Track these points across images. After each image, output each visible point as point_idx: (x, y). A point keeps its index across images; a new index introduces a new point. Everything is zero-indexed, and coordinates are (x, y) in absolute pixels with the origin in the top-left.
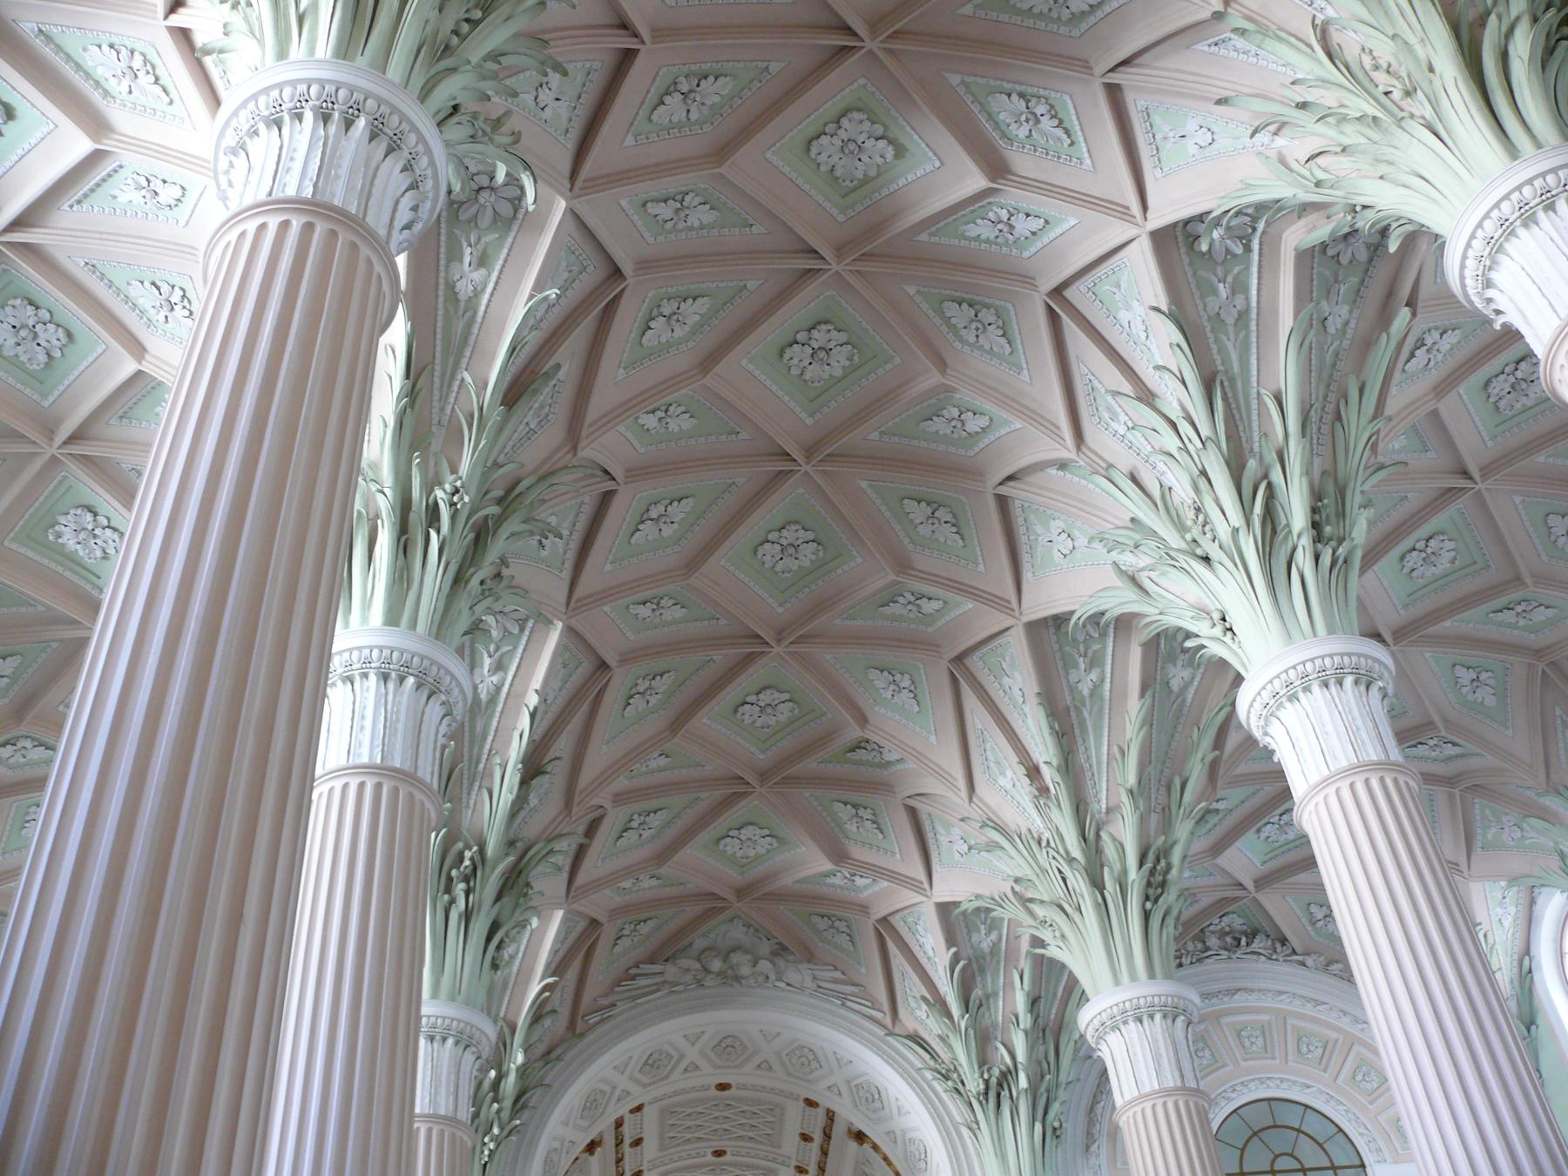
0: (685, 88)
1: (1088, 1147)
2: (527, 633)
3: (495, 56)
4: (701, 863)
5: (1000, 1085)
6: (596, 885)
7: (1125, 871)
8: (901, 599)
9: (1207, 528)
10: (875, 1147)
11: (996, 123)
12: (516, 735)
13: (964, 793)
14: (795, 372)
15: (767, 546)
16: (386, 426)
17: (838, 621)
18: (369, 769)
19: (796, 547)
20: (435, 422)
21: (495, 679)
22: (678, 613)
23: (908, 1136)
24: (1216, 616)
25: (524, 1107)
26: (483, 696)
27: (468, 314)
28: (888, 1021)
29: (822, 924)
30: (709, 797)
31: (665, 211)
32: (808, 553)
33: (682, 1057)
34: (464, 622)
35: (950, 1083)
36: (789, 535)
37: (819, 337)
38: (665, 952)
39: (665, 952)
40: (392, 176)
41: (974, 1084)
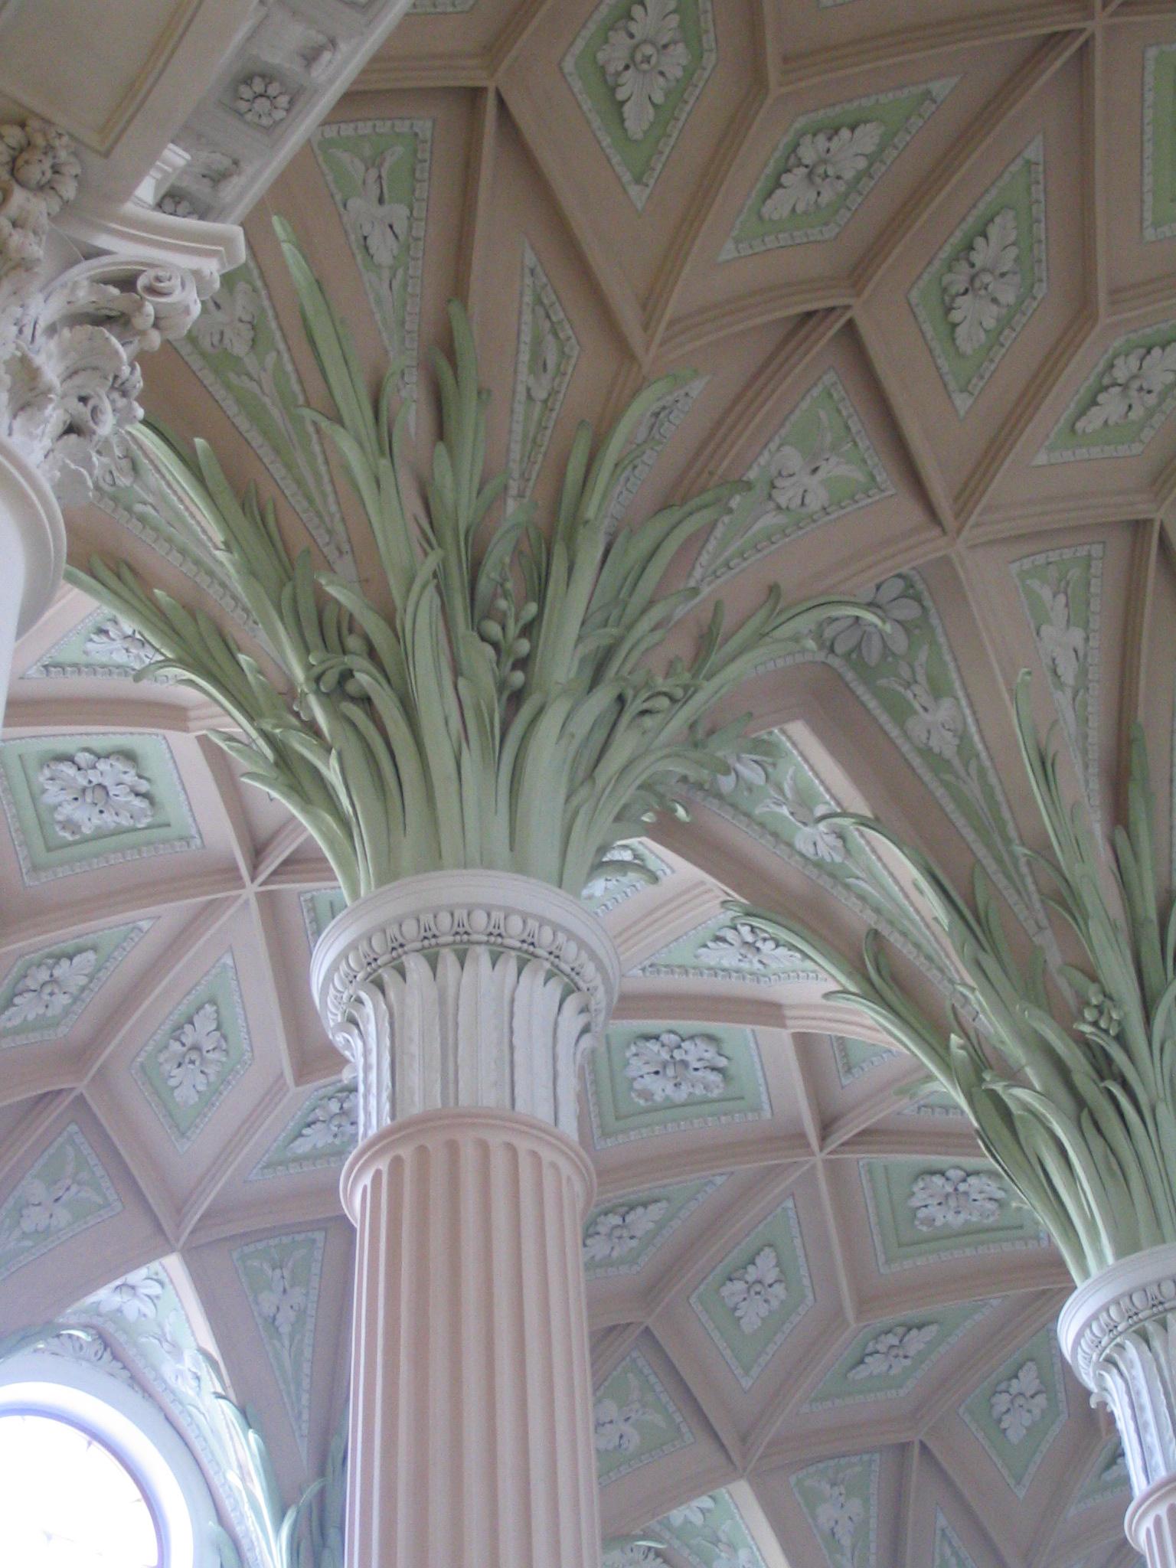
31: (1111, 406)
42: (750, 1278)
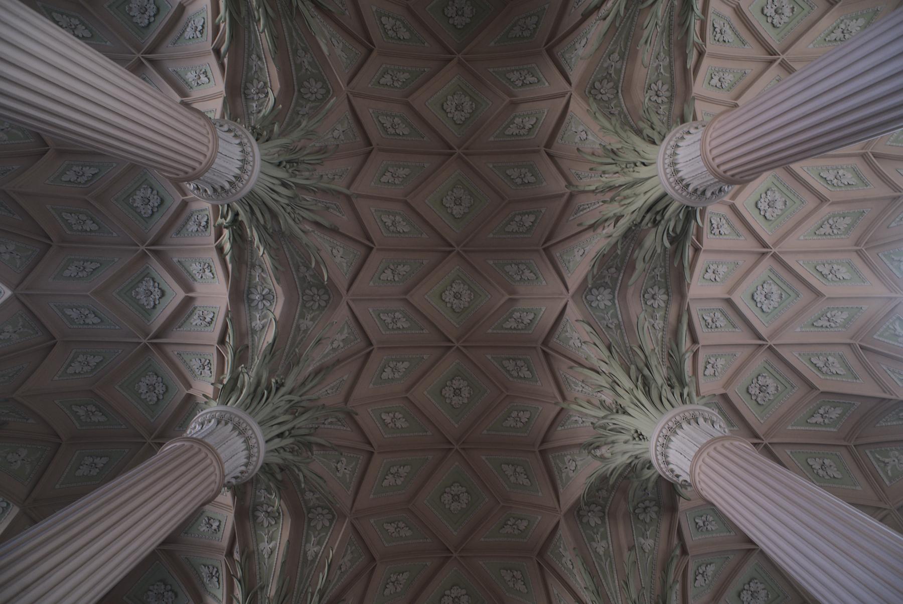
8: (509, 523)
15: (445, 495)
17: (482, 539)
19: (458, 496)
21: (315, 549)
26: (310, 558)
42: (96, 461)
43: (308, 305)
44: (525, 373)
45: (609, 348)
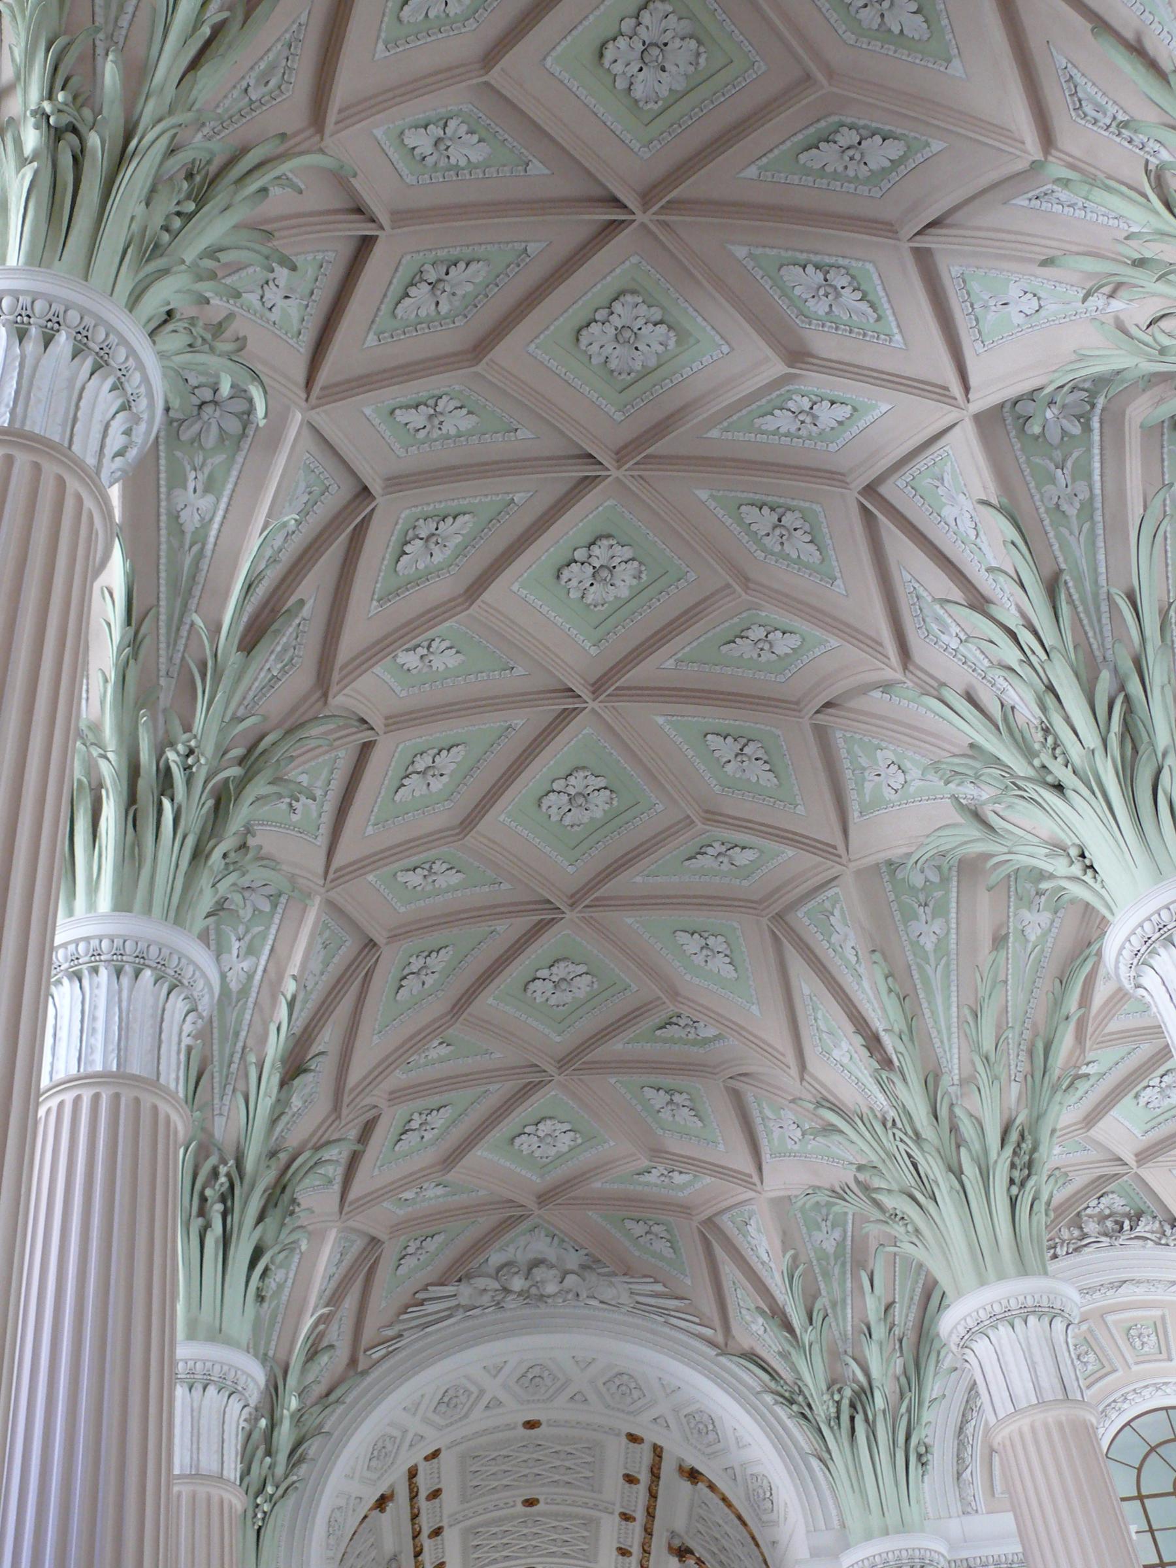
0: (432, 276)
1: (959, 1475)
2: (280, 910)
3: (212, 253)
4: (495, 1167)
5: (852, 1406)
6: (374, 1198)
7: (986, 1151)
8: (710, 850)
9: (1058, 751)
10: (712, 1487)
11: (790, 299)
12: (273, 1028)
13: (794, 1071)
14: (575, 595)
15: (552, 796)
16: (106, 681)
17: (639, 879)
18: (104, 1078)
19: (586, 797)
20: (163, 673)
21: (246, 965)
22: (454, 878)
23: (749, 1472)
24: (1074, 852)
25: (301, 1460)
26: (234, 986)
27: (196, 548)
28: (720, 1339)
29: (639, 1229)
30: (498, 1091)
31: (416, 418)
32: (600, 803)
33: (482, 1392)
34: (207, 902)
35: (795, 1407)
36: (577, 783)
37: (600, 553)
38: (459, 1271)
39: (459, 1271)
40: (101, 397)
41: (823, 1408)
43: (187, 435)
44: (799, 546)
45: (1052, 588)
